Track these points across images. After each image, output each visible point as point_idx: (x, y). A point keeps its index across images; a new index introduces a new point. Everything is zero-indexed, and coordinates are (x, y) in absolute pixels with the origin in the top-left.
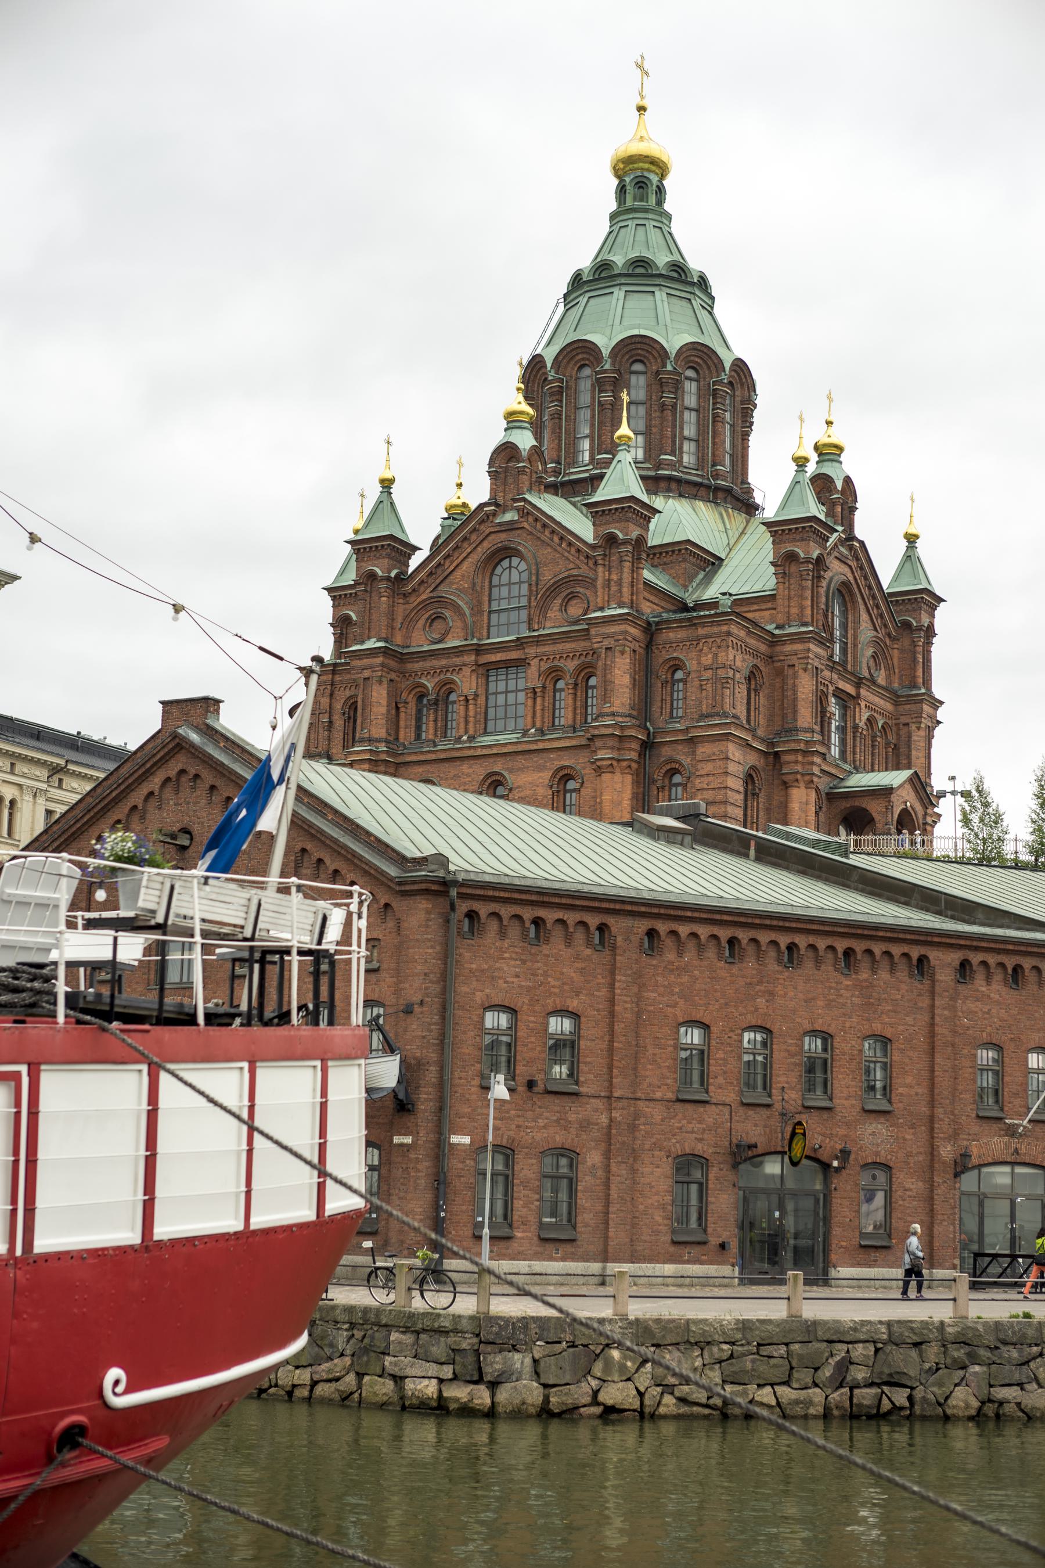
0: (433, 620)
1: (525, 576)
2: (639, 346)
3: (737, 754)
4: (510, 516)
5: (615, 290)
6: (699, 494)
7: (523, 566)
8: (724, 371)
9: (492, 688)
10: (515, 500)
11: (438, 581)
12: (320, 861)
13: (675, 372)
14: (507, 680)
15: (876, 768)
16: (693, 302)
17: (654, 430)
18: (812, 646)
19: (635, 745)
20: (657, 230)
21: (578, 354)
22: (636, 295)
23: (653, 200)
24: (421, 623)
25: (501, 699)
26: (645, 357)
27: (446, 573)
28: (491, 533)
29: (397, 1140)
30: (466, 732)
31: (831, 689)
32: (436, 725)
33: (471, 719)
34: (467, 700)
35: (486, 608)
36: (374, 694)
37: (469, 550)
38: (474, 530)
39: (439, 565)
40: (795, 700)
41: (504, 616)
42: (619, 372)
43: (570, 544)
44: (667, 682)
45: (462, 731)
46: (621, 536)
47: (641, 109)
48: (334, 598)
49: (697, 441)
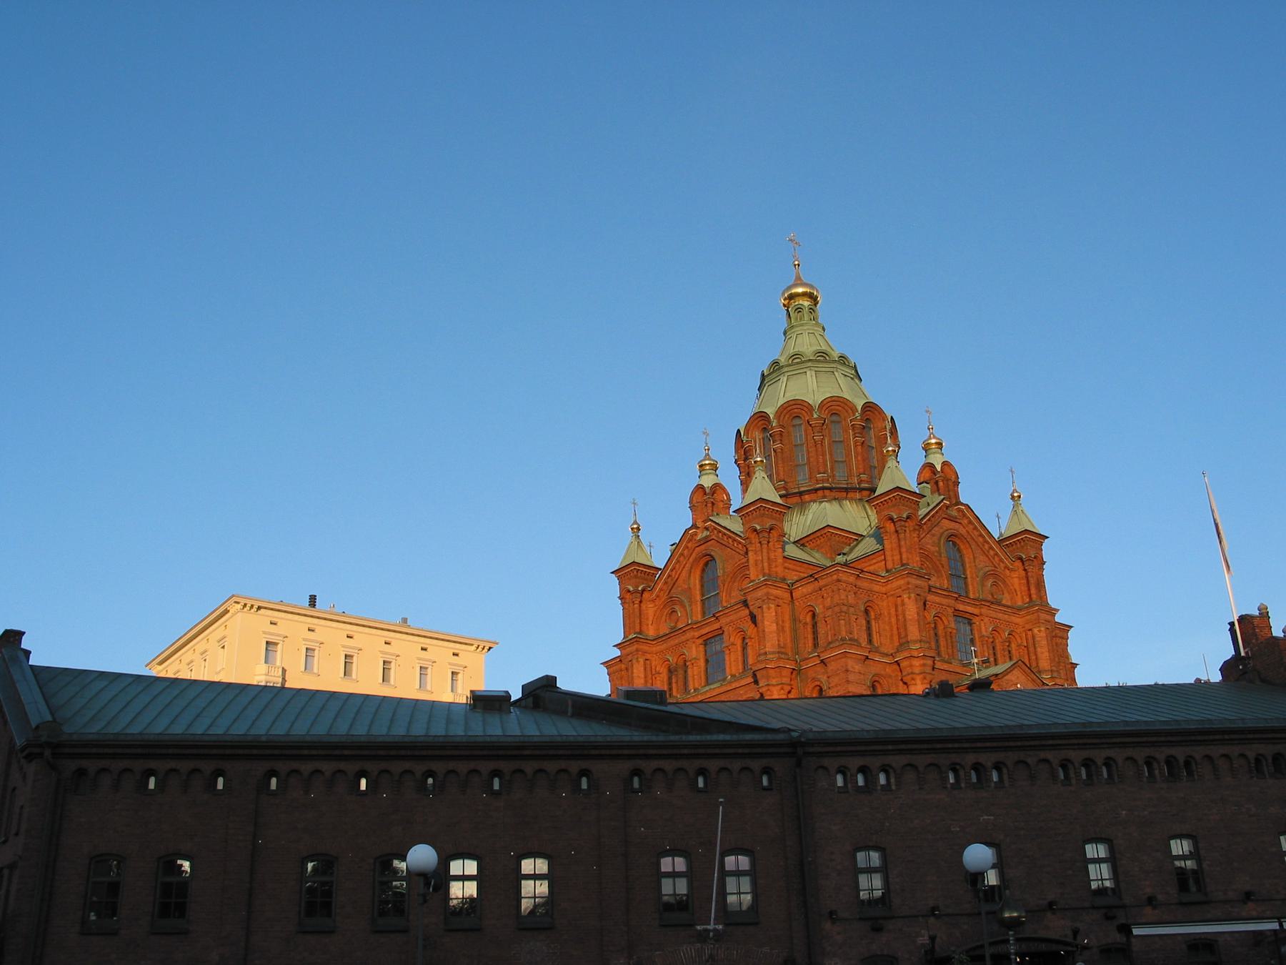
2: (794, 407)
3: (857, 667)
4: (706, 533)
5: (781, 377)
6: (849, 496)
8: (857, 411)
10: (705, 521)
13: (820, 418)
16: (835, 373)
17: (811, 459)
18: (910, 579)
19: (786, 673)
21: (759, 422)
24: (664, 618)
26: (800, 413)
31: (950, 611)
32: (677, 685)
36: (635, 671)
39: (669, 576)
42: (782, 426)
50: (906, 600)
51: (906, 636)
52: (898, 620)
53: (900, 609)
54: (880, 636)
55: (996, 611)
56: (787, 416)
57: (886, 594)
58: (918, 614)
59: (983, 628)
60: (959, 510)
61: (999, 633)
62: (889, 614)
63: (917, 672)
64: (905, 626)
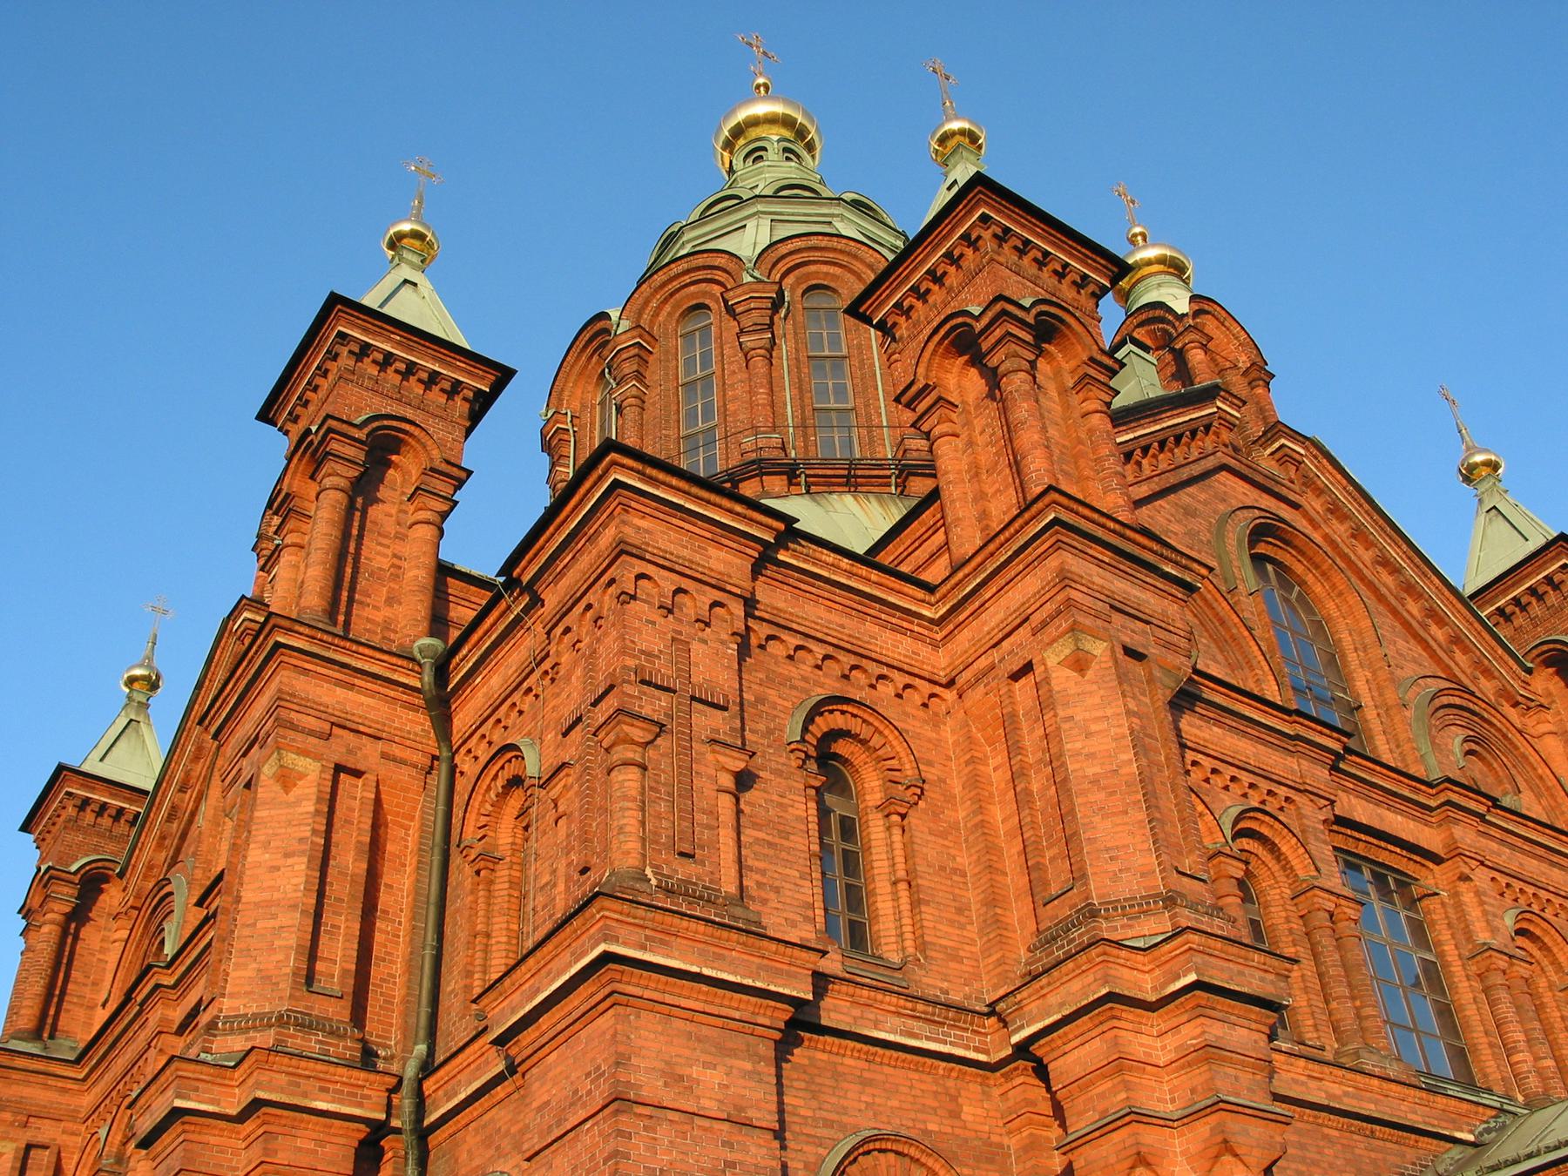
2: (687, 279)
3: (714, 1077)
50: (1062, 679)
51: (1079, 876)
52: (1022, 800)
53: (1031, 738)
54: (915, 904)
55: (1512, 846)
56: (668, 308)
57: (950, 684)
58: (1139, 745)
59: (1474, 913)
60: (1283, 457)
61: (1544, 947)
62: (975, 781)
63: (1169, 1109)
64: (1065, 815)
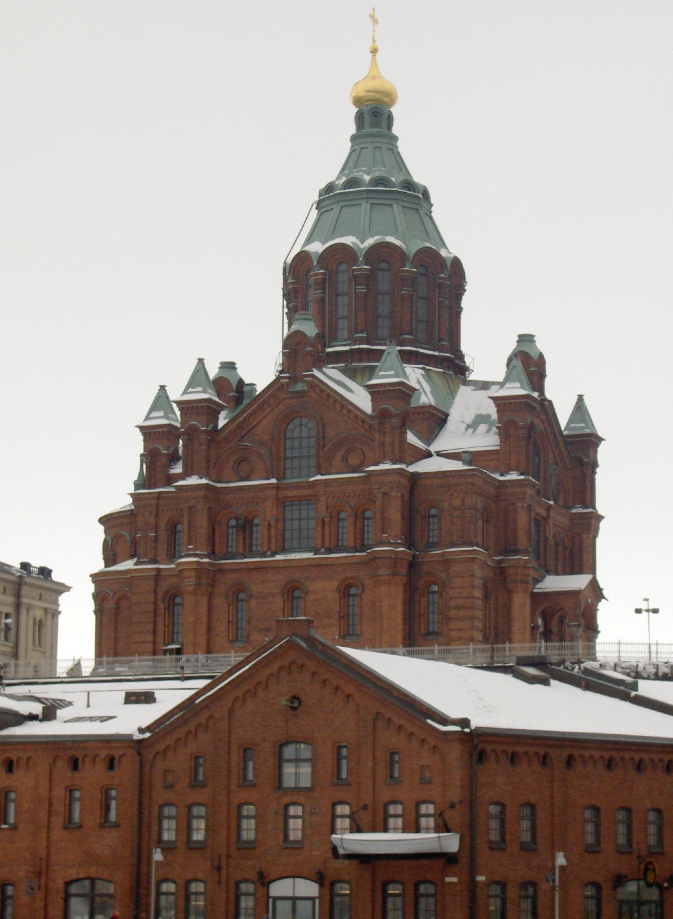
0: (240, 463)
1: (313, 433)
4: (299, 387)
7: (311, 425)
8: (447, 268)
9: (288, 515)
11: (244, 433)
12: (389, 720)
14: (300, 510)
15: (560, 568)
20: (390, 151)
22: (380, 207)
23: (384, 125)
25: (296, 524)
27: (251, 426)
28: (285, 399)
29: (448, 880)
30: (269, 549)
33: (273, 539)
34: (269, 525)
35: (282, 454)
37: (268, 411)
38: (272, 395)
40: (515, 529)
41: (296, 463)
43: (349, 411)
44: (425, 517)
45: (265, 548)
46: (392, 410)
47: (374, 51)
48: (144, 434)
49: (427, 322)
